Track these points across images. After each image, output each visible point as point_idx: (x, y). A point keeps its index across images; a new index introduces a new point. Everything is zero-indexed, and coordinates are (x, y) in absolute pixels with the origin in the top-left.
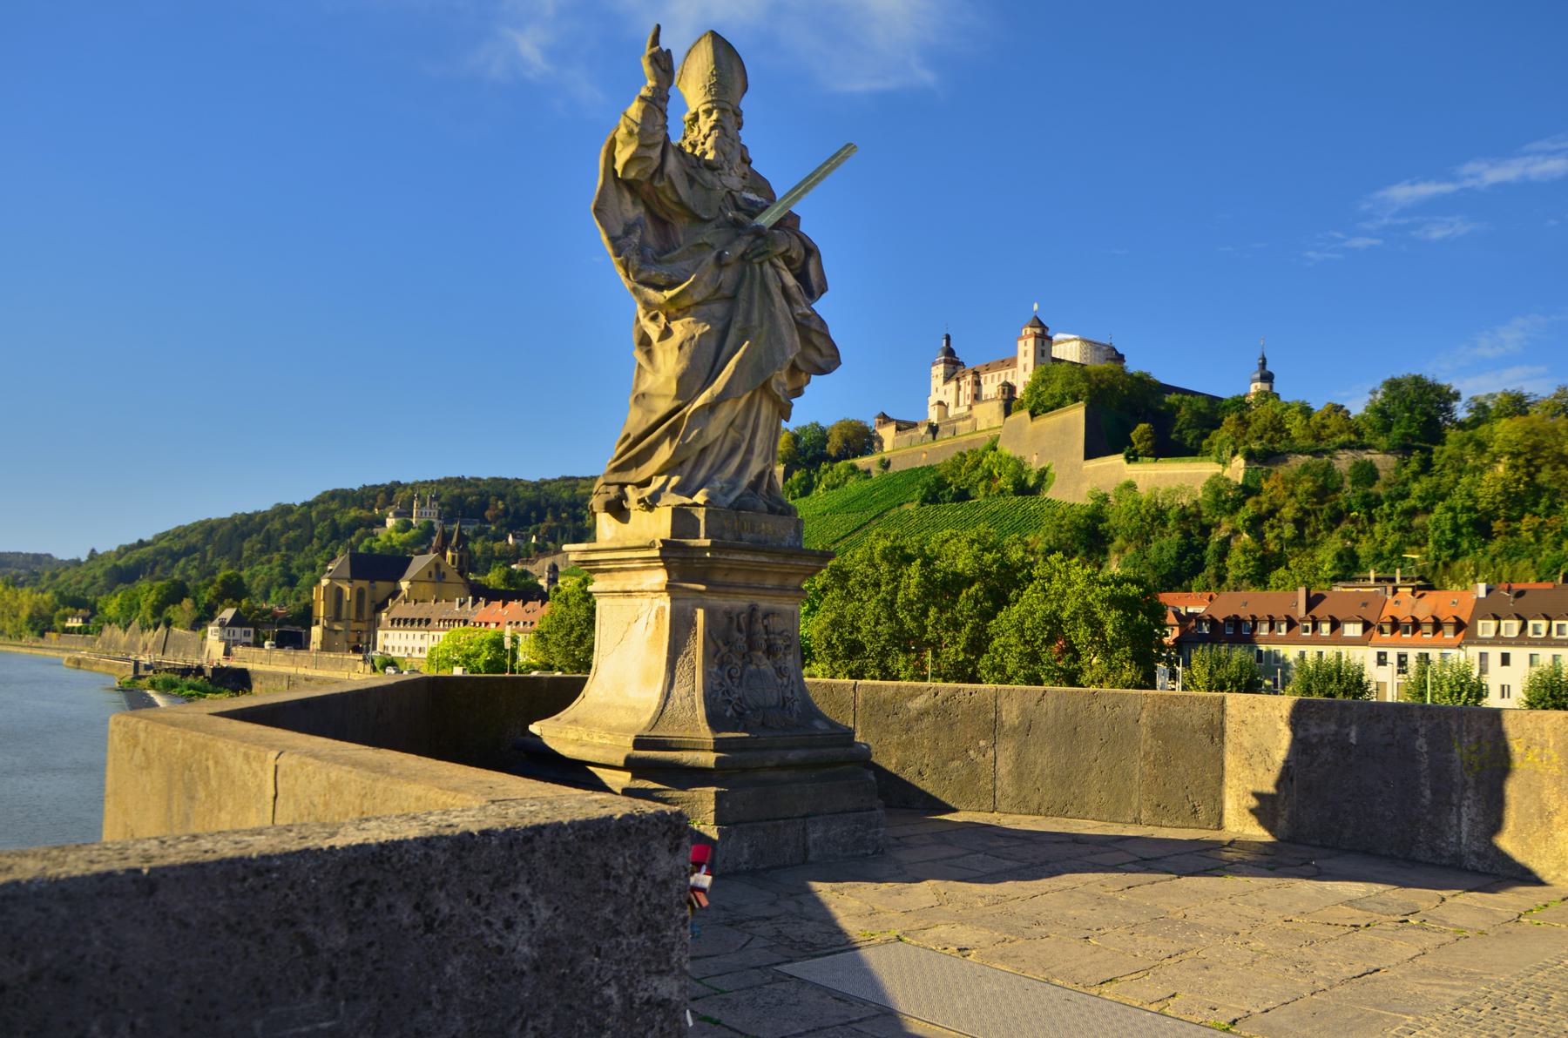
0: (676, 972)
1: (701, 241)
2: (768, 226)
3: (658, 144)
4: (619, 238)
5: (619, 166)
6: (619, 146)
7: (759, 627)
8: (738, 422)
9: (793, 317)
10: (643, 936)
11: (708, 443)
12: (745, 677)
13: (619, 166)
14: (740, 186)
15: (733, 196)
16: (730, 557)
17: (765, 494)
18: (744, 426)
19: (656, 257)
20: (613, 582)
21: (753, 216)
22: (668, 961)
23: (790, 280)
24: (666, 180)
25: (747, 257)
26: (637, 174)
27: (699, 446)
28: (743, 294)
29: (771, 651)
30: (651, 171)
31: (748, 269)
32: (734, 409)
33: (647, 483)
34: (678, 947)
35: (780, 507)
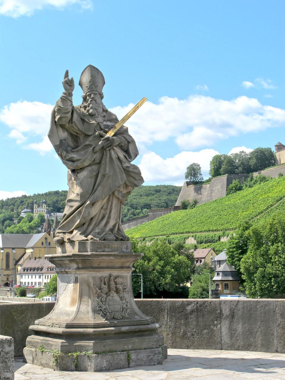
0: (11, 372)
1: (87, 144)
3: (69, 112)
5: (56, 120)
6: (56, 114)
7: (112, 283)
8: (104, 207)
10: (3, 364)
12: (107, 301)
13: (56, 120)
15: (100, 125)
18: (106, 209)
19: (72, 150)
20: (61, 268)
21: (106, 132)
22: (9, 370)
23: (121, 155)
25: (104, 148)
28: (103, 162)
29: (117, 291)
31: (105, 152)
32: (102, 203)
34: (11, 366)
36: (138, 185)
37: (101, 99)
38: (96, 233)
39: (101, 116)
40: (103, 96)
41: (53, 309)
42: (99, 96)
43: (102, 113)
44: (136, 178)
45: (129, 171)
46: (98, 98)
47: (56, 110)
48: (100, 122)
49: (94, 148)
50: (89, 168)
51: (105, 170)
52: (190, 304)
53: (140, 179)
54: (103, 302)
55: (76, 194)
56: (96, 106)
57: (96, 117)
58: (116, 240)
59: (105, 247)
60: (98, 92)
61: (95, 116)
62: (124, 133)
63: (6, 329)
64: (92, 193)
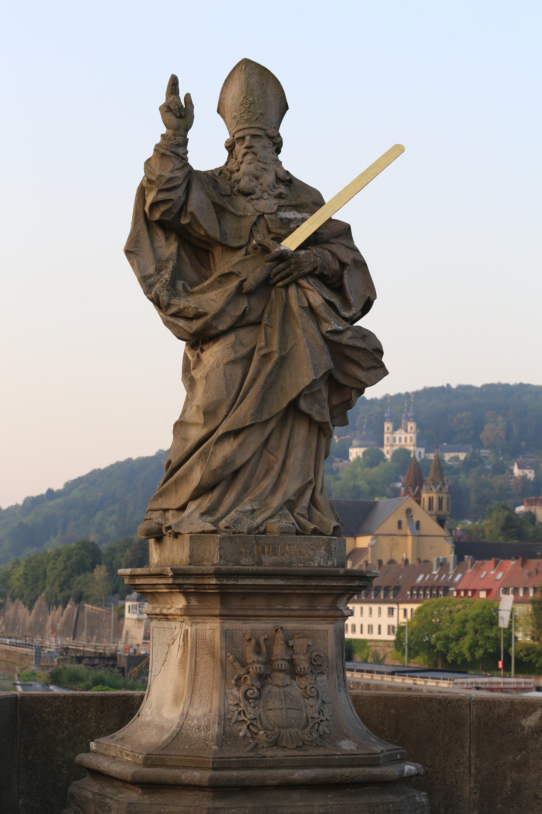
1: (227, 271)
2: (293, 248)
4: (151, 276)
9: (323, 336)
11: (235, 467)
14: (276, 208)
16: (240, 582)
17: (304, 512)
19: (189, 288)
21: (279, 239)
24: (190, 216)
26: (161, 215)
27: (228, 472)
30: (175, 211)
33: (183, 508)
35: (312, 526)
36: (368, 382)
37: (272, 149)
38: (244, 512)
39: (269, 194)
40: (281, 142)
41: (137, 714)
42: (266, 141)
43: (274, 186)
44: (363, 363)
45: (340, 344)
46: (265, 148)
47: (145, 184)
48: (267, 211)
49: (243, 282)
50: (231, 338)
51: (268, 344)
52: (532, 713)
53: (374, 367)
54: (250, 701)
55: (194, 408)
56: (257, 170)
57: (257, 199)
58: (298, 533)
59: (264, 552)
60: (264, 130)
61: (253, 197)
62: (331, 241)
63: (30, 758)
64: (235, 405)
